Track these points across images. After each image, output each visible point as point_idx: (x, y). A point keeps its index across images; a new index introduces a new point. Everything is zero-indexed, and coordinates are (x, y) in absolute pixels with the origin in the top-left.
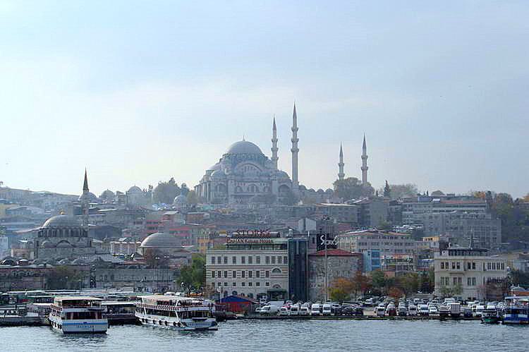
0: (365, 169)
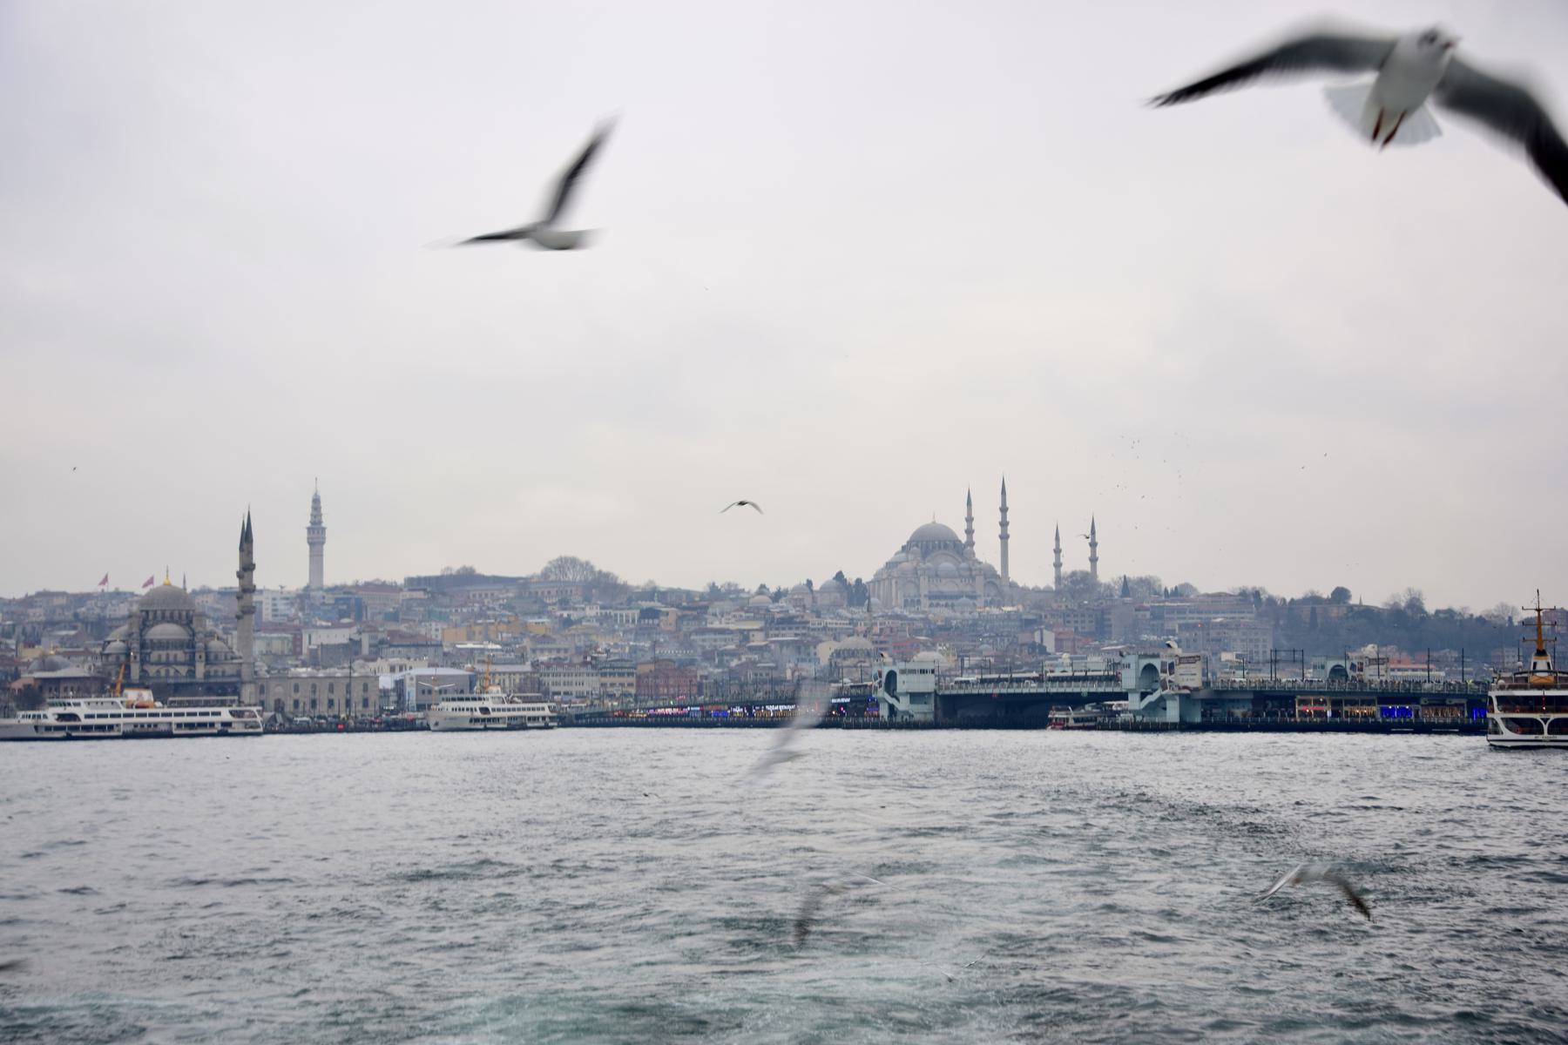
0: (1093, 560)
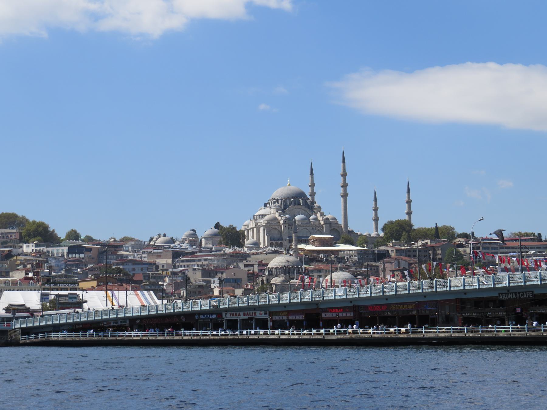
0: (409, 213)
